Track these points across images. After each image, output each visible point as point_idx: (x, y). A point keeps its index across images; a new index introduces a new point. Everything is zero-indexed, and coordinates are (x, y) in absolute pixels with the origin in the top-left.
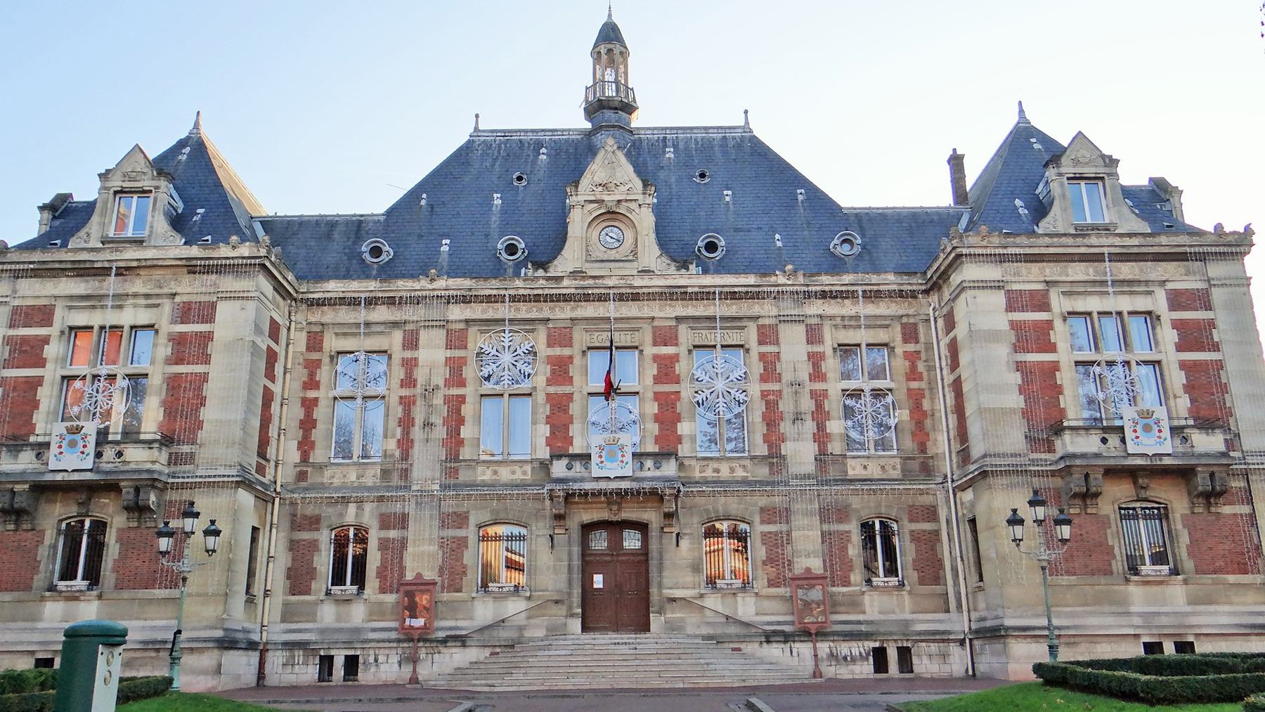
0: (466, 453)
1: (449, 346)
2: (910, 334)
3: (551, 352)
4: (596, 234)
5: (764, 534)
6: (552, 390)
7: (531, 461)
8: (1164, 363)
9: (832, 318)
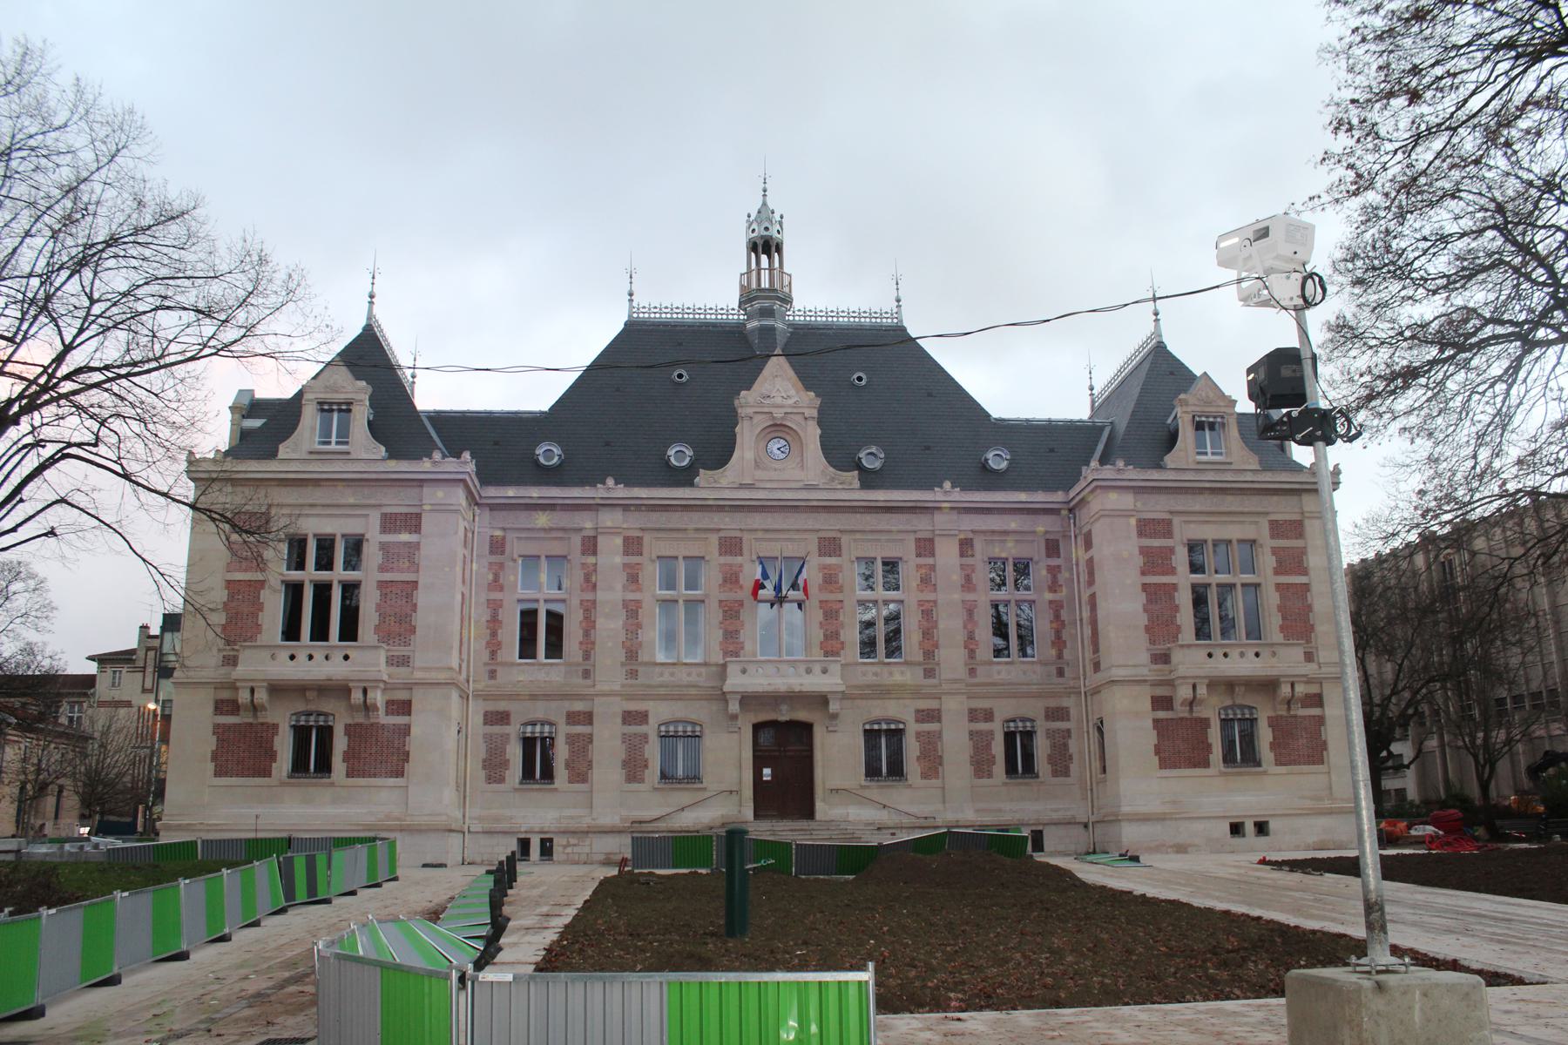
0: (644, 657)
1: (626, 553)
2: (1052, 548)
3: (723, 560)
4: (762, 444)
5: (918, 735)
6: (723, 597)
7: (705, 664)
8: (1263, 587)
9: (984, 532)
